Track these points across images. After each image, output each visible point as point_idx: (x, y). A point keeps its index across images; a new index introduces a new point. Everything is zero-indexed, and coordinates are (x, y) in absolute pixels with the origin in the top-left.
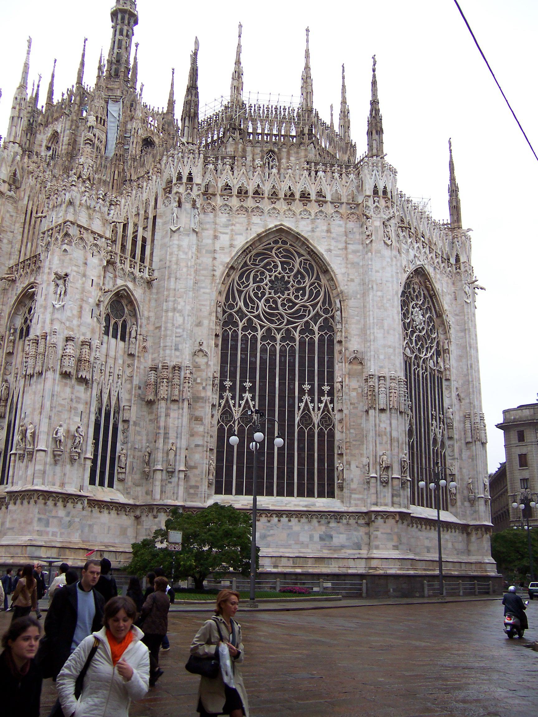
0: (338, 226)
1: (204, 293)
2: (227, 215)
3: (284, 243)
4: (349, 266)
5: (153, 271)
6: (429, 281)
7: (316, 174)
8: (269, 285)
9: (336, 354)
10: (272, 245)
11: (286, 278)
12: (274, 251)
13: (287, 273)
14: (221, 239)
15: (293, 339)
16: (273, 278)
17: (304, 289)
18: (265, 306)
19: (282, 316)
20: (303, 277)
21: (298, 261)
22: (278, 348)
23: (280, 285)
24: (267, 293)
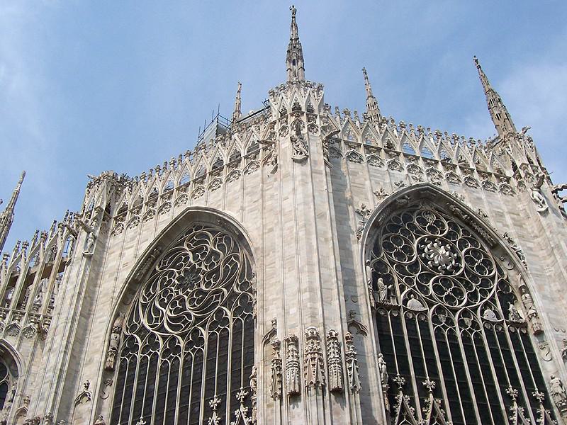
5: (51, 318)
6: (452, 203)
11: (197, 267)
12: (185, 245)
18: (171, 311)
19: (189, 315)
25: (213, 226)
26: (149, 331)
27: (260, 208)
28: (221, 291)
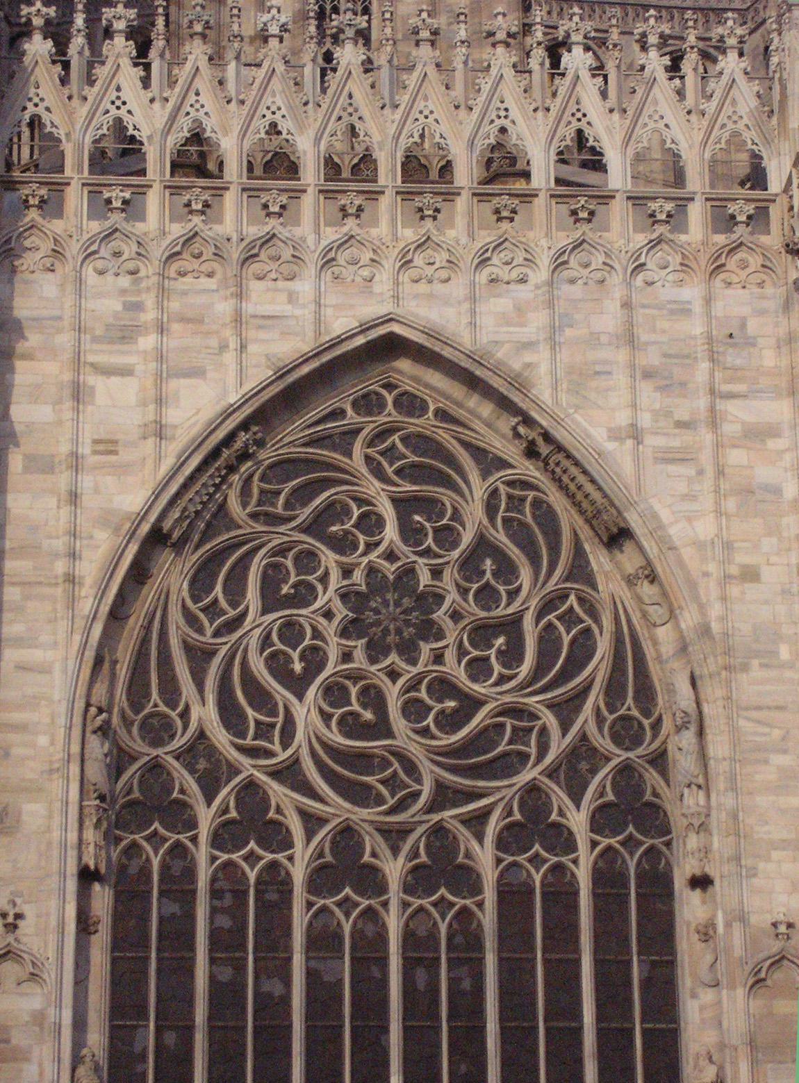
0: (683, 306)
1: (22, 668)
2: (125, 281)
3: (411, 404)
4: (731, 504)
7: (555, 62)
8: (342, 612)
9: (687, 945)
10: (352, 417)
11: (424, 578)
13: (427, 553)
14: (101, 398)
15: (466, 880)
16: (358, 576)
17: (512, 626)
18: (326, 717)
19: (411, 768)
20: (506, 570)
21: (479, 489)
22: (394, 924)
23: (391, 615)
24: (333, 654)
25: (478, 425)
26: (234, 770)
27: (706, 458)
28: (534, 717)
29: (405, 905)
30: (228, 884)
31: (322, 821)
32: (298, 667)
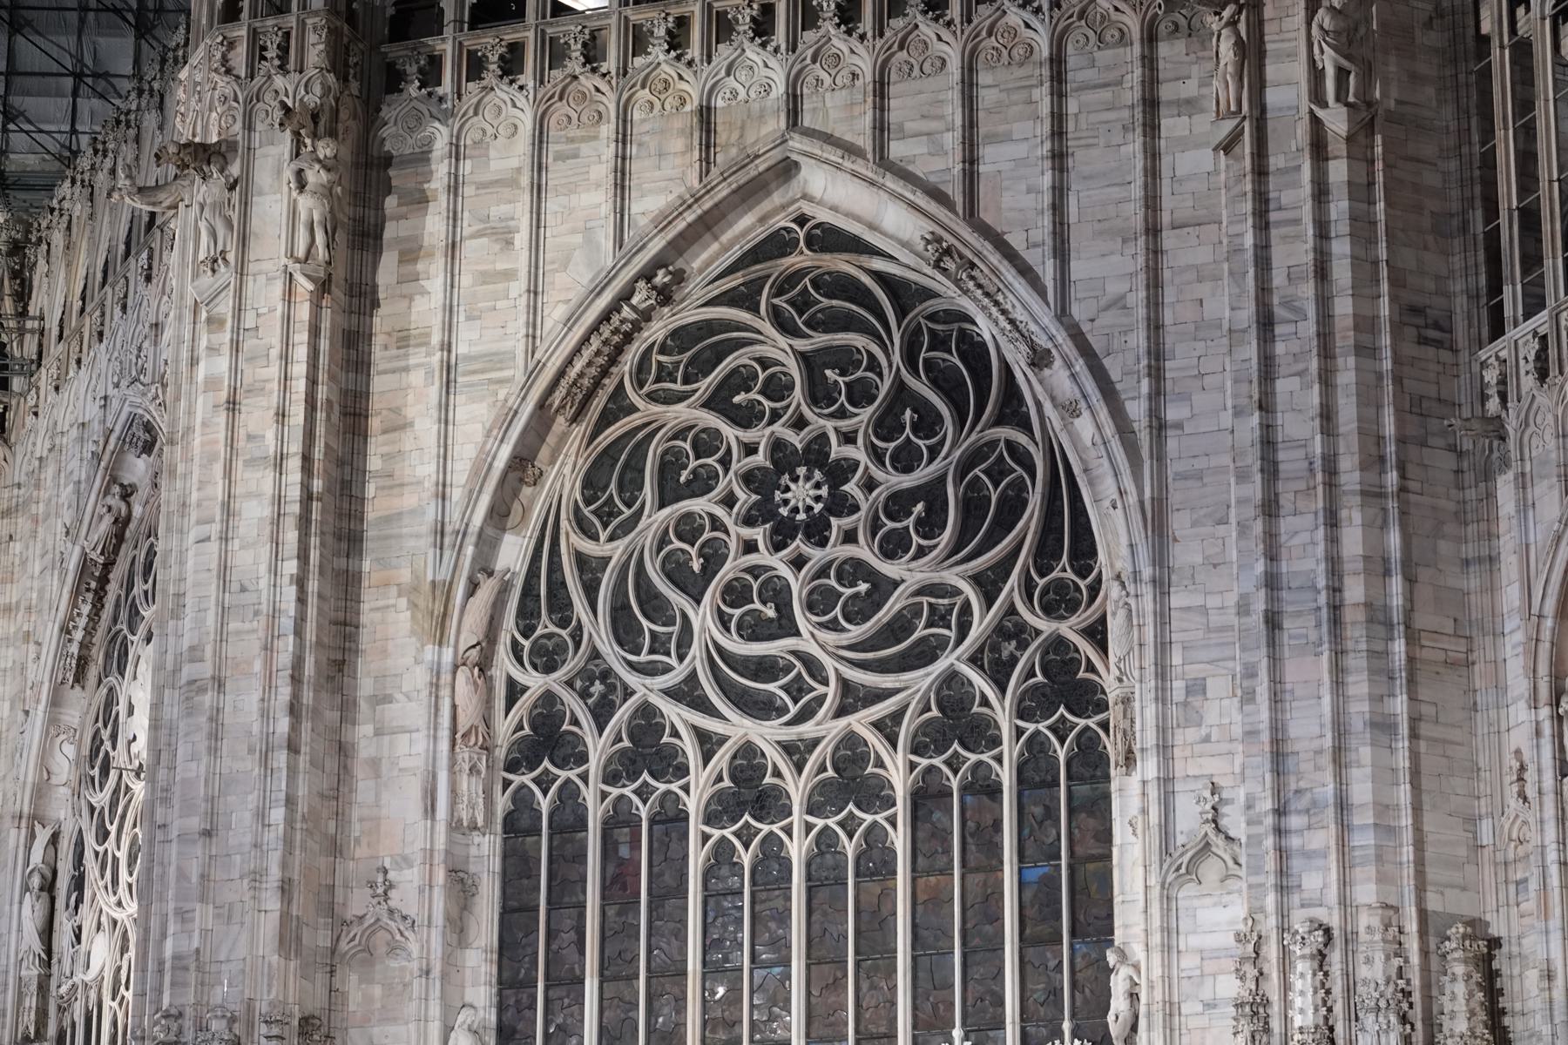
18: (724, 621)
20: (928, 423)
22: (797, 850)
26: (628, 693)
29: (809, 827)
30: (619, 821)
31: (723, 740)
32: (696, 565)
